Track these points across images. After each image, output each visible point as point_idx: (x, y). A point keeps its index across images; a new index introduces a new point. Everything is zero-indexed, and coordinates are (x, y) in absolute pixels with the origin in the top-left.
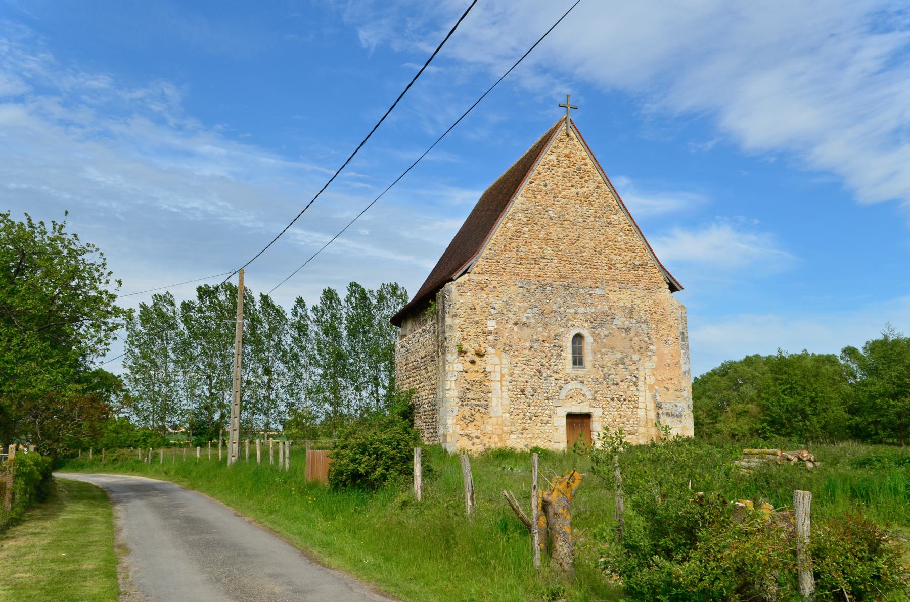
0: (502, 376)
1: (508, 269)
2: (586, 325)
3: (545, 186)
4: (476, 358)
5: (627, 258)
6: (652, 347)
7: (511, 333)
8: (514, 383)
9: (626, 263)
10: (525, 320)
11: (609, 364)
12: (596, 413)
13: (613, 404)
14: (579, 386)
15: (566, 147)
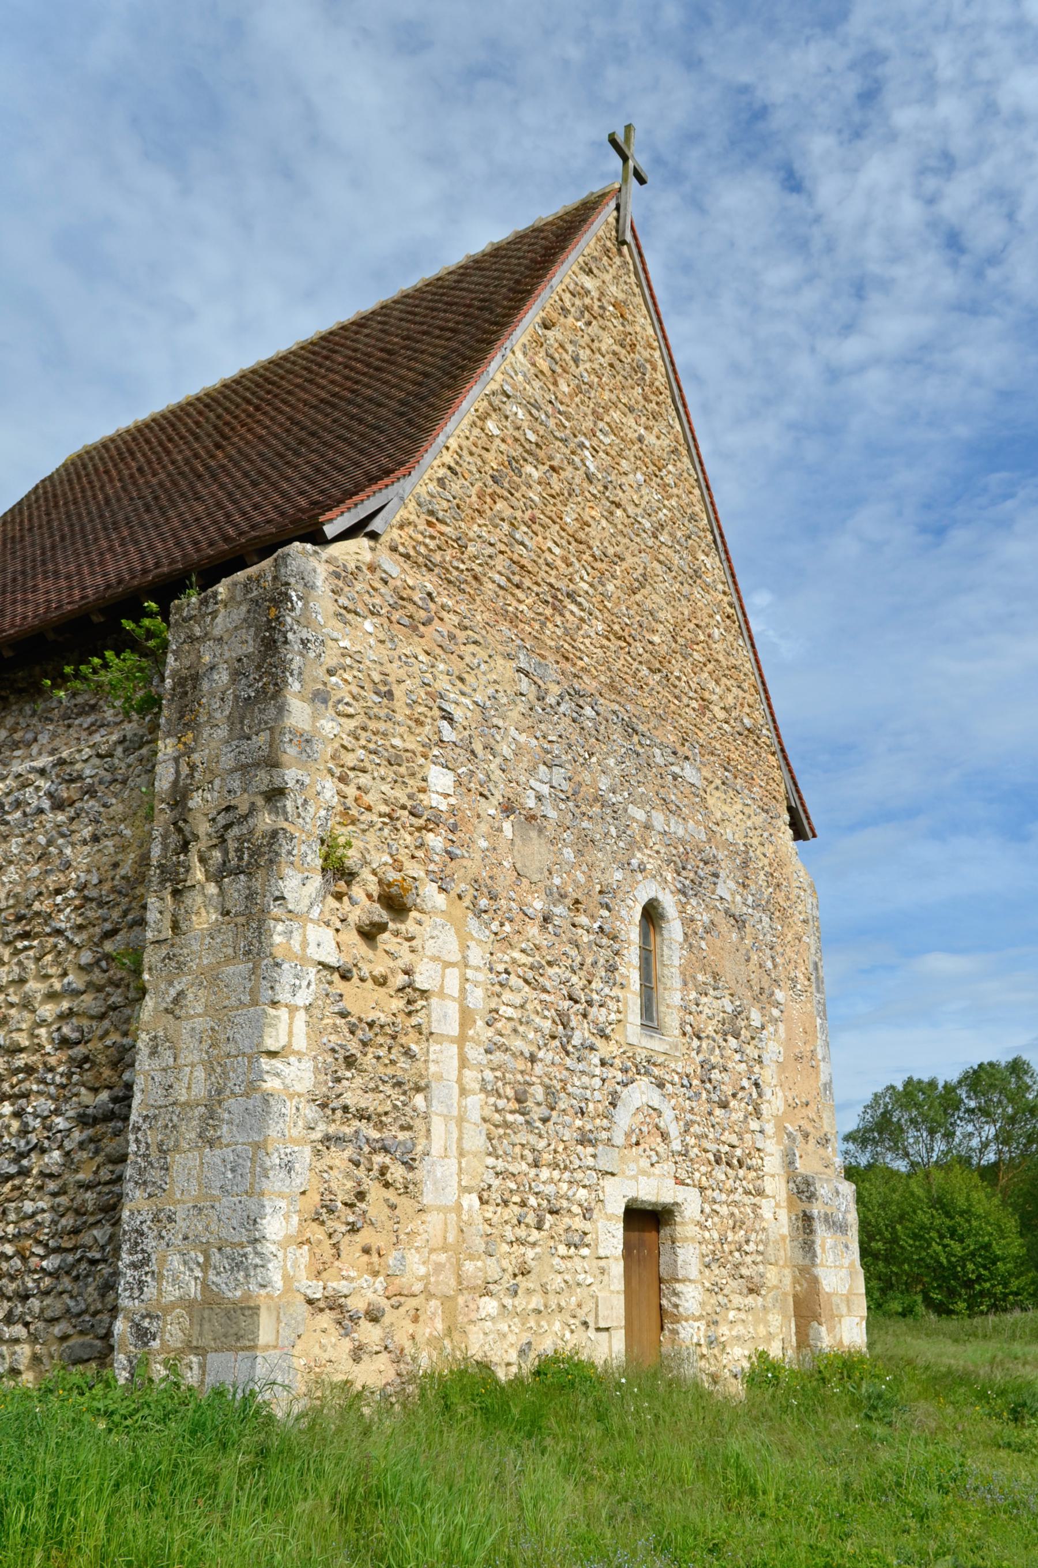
0: (466, 1017)
8: (498, 1057)
12: (691, 1204)
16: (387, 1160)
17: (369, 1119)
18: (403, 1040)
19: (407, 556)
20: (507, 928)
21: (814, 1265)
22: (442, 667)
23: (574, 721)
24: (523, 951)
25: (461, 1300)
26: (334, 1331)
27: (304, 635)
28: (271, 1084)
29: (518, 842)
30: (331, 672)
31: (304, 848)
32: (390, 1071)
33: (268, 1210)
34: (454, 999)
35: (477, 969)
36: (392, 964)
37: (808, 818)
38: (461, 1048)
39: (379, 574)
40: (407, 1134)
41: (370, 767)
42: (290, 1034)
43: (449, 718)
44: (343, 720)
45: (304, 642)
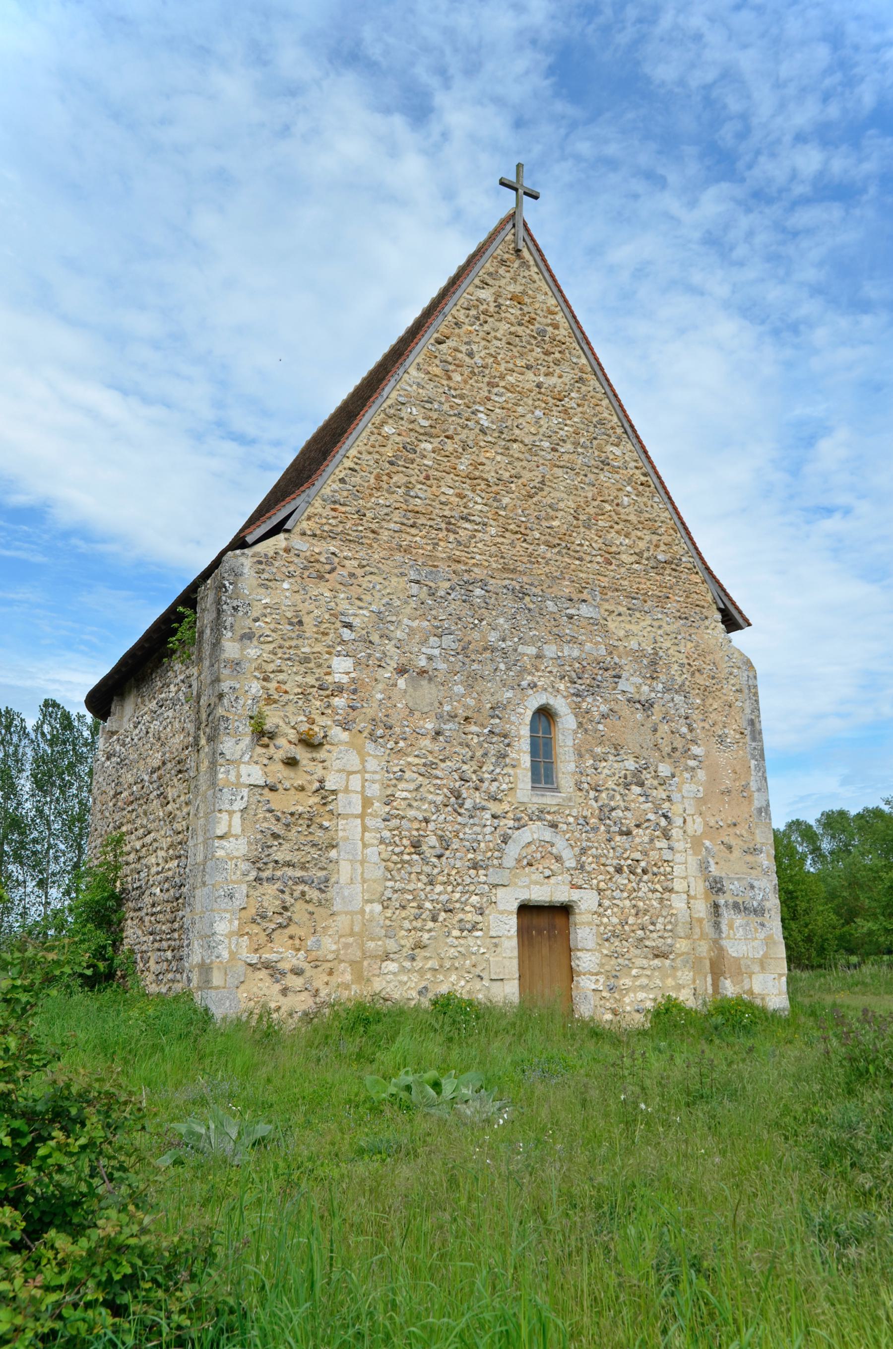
0: (367, 802)
1: (385, 535)
2: (562, 687)
3: (471, 355)
4: (301, 753)
5: (642, 545)
6: (696, 750)
7: (389, 692)
8: (395, 822)
9: (640, 554)
10: (423, 662)
11: (610, 784)
12: (586, 902)
13: (622, 880)
14: (548, 834)
15: (514, 280)
16: (306, 889)
17: (293, 866)
18: (318, 820)
19: (315, 535)
20: (402, 744)
21: (721, 938)
22: (342, 596)
23: (464, 601)
24: (416, 756)
25: (365, 963)
26: (268, 981)
27: (235, 603)
28: (220, 853)
29: (410, 690)
30: (256, 620)
31: (236, 724)
32: (310, 838)
33: (217, 919)
34: (357, 792)
35: (375, 772)
36: (309, 778)
37: (740, 612)
38: (363, 821)
39: (293, 552)
40: (324, 873)
41: (284, 668)
42: (230, 826)
43: (349, 626)
44: (263, 646)
45: (235, 609)
